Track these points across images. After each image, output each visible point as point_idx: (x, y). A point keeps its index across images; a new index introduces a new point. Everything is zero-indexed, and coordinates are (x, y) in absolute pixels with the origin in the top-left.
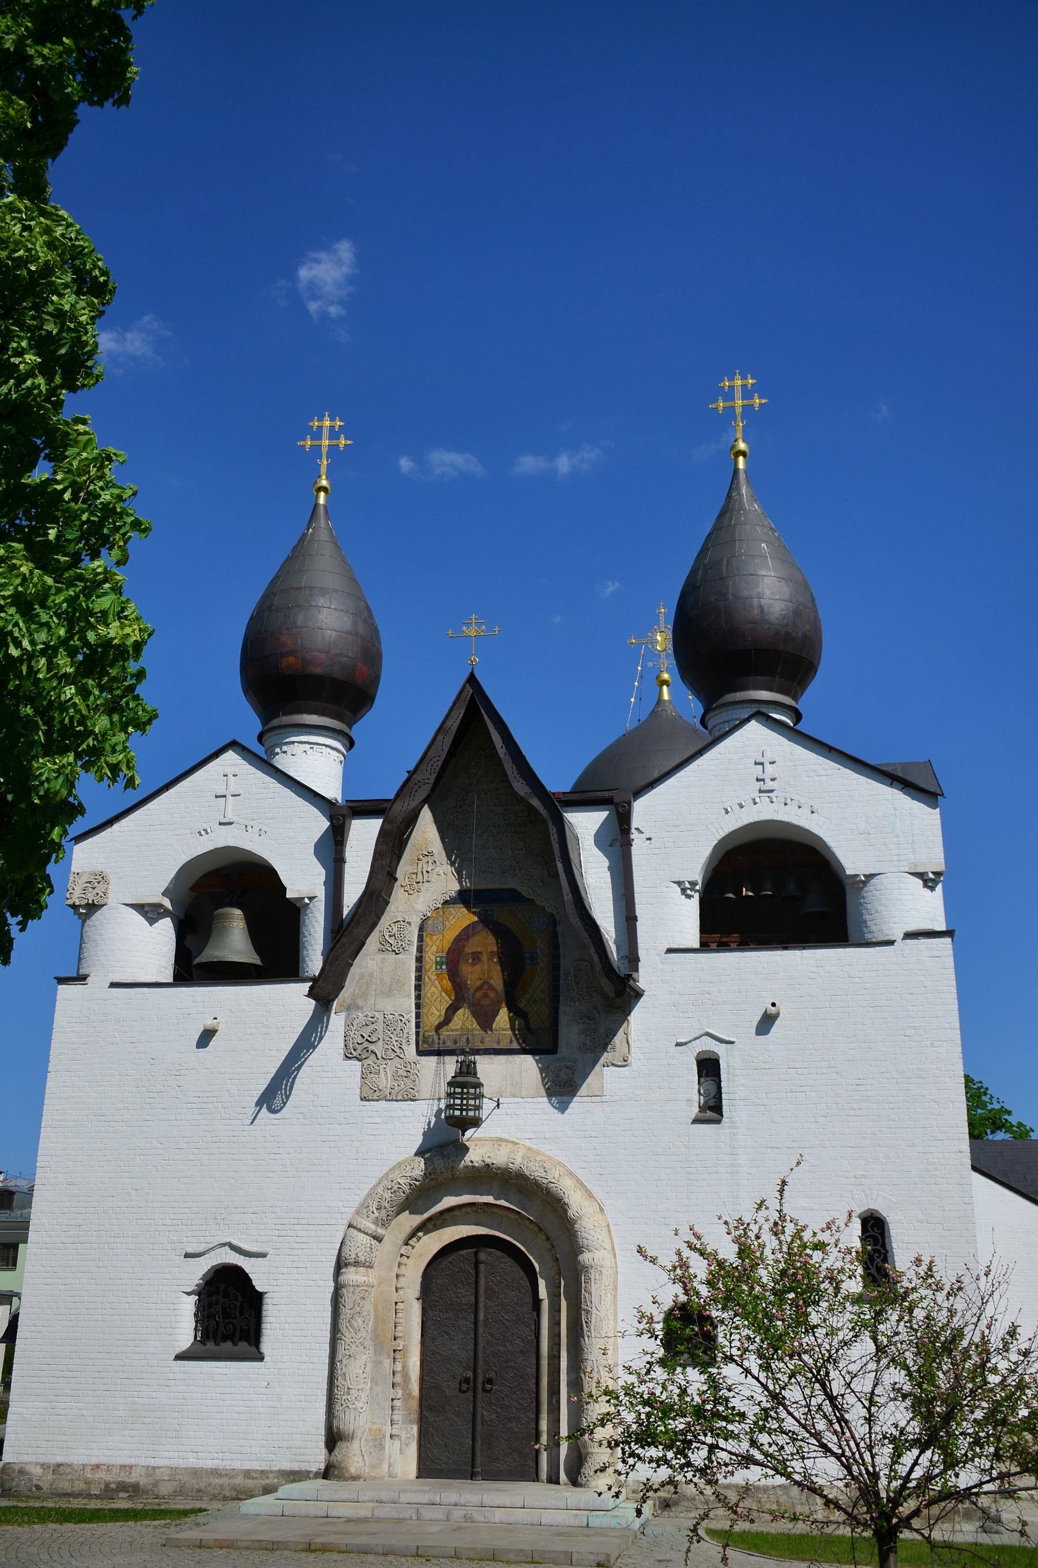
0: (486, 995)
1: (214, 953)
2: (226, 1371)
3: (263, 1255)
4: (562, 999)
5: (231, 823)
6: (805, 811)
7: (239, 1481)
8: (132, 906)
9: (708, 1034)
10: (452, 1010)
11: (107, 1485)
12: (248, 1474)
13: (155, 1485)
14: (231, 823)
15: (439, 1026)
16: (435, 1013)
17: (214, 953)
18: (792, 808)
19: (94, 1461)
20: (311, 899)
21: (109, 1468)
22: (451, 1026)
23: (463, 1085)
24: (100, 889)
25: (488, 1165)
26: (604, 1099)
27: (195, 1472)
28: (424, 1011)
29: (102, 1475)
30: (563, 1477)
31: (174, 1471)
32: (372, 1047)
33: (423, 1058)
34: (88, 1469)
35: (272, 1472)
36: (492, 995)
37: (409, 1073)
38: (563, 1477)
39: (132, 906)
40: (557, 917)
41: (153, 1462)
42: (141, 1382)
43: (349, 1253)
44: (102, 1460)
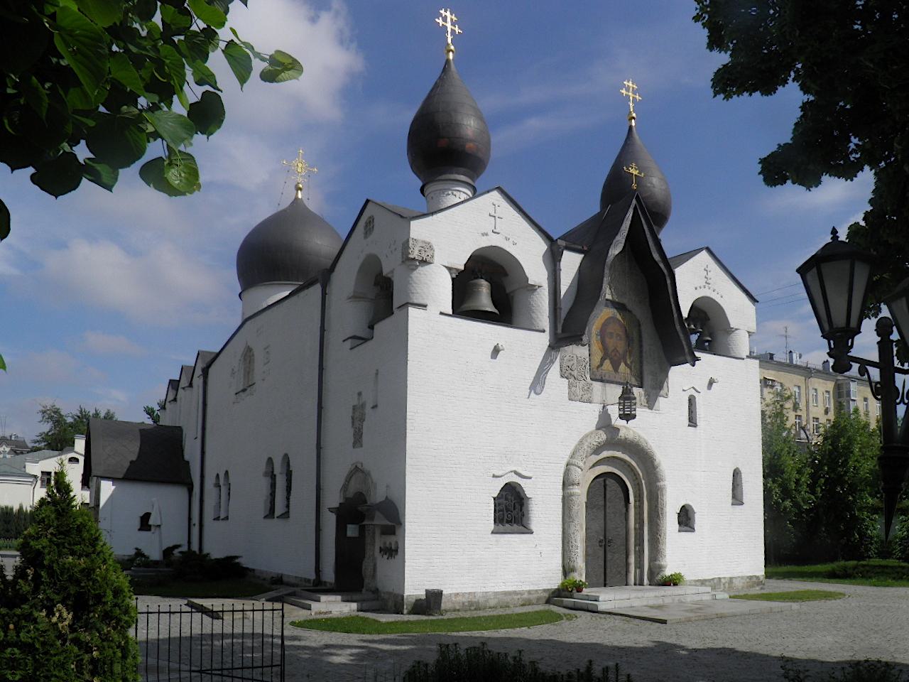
0: (615, 355)
1: (471, 305)
2: (516, 539)
3: (530, 478)
4: (645, 363)
5: (498, 233)
6: (719, 296)
7: (526, 596)
8: (446, 267)
9: (693, 388)
10: (603, 360)
11: (463, 603)
12: (529, 592)
13: (487, 601)
14: (498, 233)
15: (598, 367)
16: (597, 360)
17: (471, 305)
18: (715, 293)
19: (455, 591)
20: (539, 287)
21: (464, 594)
22: (603, 367)
23: (625, 399)
24: (430, 253)
25: (626, 439)
26: (660, 412)
27: (506, 593)
28: (592, 358)
29: (460, 599)
30: (646, 581)
31: (496, 593)
32: (573, 373)
33: (594, 382)
34: (453, 596)
35: (540, 590)
36: (618, 354)
37: (589, 389)
38: (646, 581)
39: (446, 267)
40: (641, 323)
41: (484, 590)
42: (475, 546)
43: (574, 477)
44: (459, 591)
